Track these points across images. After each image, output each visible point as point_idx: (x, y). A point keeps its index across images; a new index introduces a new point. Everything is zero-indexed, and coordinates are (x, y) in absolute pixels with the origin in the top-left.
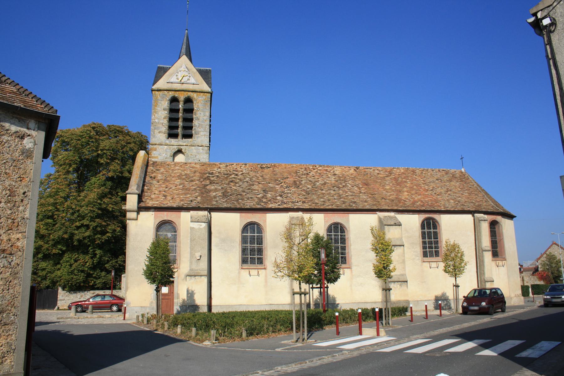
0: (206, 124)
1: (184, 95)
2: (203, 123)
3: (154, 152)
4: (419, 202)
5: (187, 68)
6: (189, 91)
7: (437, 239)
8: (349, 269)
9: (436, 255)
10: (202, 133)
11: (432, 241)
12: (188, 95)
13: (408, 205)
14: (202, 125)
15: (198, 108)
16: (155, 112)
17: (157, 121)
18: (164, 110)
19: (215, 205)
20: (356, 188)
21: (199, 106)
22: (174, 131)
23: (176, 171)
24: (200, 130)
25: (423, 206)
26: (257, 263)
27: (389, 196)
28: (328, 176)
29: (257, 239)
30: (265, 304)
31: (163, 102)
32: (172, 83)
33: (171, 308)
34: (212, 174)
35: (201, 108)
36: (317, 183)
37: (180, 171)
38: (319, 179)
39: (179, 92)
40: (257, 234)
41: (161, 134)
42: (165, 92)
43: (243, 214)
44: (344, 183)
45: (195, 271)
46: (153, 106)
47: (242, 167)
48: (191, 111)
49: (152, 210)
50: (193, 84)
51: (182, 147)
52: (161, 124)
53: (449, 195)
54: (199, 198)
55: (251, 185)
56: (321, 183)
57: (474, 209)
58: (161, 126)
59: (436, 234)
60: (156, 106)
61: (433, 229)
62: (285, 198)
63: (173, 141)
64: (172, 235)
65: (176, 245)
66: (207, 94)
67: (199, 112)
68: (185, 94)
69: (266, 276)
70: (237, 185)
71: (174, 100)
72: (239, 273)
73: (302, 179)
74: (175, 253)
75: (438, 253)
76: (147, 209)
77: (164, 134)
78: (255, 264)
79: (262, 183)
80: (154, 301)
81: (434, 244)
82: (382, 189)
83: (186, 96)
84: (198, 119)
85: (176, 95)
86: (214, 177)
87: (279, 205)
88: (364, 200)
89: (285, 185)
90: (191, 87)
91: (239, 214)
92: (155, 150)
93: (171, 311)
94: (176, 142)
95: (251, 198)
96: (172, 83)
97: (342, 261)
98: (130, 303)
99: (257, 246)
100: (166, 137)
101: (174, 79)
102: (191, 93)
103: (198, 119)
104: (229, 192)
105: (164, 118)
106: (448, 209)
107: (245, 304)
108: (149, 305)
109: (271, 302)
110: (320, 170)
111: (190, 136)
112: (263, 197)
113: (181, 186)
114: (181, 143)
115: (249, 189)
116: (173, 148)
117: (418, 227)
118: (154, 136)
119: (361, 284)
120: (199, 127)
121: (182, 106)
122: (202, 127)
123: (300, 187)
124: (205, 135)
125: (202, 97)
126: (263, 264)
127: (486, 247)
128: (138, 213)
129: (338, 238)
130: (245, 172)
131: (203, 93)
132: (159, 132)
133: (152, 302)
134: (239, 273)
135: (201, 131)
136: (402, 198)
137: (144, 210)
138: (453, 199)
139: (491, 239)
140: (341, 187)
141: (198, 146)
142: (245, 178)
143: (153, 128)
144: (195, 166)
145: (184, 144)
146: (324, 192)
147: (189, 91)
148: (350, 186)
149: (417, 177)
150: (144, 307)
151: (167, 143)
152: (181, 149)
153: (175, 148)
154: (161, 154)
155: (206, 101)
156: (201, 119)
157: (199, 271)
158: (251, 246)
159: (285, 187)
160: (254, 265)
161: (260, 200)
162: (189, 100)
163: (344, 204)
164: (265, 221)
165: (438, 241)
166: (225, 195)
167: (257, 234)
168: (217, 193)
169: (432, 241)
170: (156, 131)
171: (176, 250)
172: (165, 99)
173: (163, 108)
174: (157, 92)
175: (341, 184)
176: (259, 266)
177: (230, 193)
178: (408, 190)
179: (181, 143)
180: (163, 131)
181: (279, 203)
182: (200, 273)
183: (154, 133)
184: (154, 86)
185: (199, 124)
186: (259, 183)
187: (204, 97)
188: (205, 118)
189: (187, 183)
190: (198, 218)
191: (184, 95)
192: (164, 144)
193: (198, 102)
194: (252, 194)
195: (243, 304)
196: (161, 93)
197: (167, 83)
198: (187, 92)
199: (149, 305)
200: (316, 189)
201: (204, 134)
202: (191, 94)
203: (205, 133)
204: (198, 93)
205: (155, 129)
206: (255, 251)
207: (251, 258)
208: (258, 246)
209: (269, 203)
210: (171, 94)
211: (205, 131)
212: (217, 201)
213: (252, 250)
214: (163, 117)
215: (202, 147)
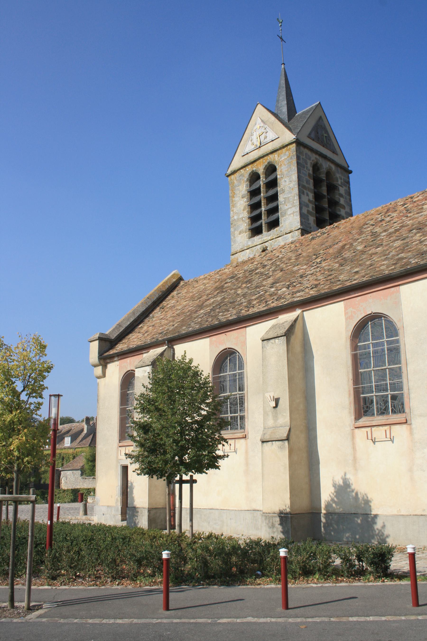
1: (263, 163)
6: (267, 155)
8: (405, 426)
10: (290, 212)
12: (268, 161)
14: (289, 197)
15: (282, 174)
16: (233, 206)
17: (236, 217)
18: (243, 198)
21: (283, 170)
22: (258, 224)
30: (246, 509)
31: (240, 187)
32: (247, 154)
35: (285, 173)
39: (257, 162)
41: (242, 235)
42: (242, 170)
43: (214, 338)
46: (230, 198)
49: (116, 359)
50: (272, 141)
51: (266, 244)
52: (241, 221)
58: (241, 222)
60: (233, 197)
63: (256, 240)
66: (291, 146)
67: (283, 180)
68: (264, 161)
69: (247, 452)
76: (111, 358)
77: (246, 232)
83: (266, 163)
84: (283, 191)
85: (254, 169)
91: (208, 340)
94: (259, 239)
96: (247, 154)
97: (394, 406)
100: (248, 236)
102: (271, 156)
105: (244, 210)
107: (218, 507)
108: (114, 505)
114: (265, 238)
116: (256, 249)
120: (285, 203)
121: (263, 181)
124: (293, 213)
125: (285, 155)
128: (105, 367)
129: (383, 350)
131: (285, 148)
135: (288, 209)
141: (286, 234)
143: (233, 230)
145: (269, 238)
147: (267, 155)
150: (110, 506)
151: (249, 245)
152: (267, 247)
153: (259, 248)
155: (291, 158)
156: (287, 189)
164: (244, 343)
170: (237, 233)
172: (242, 182)
173: (241, 196)
174: (232, 177)
180: (244, 229)
183: (234, 237)
184: (229, 170)
185: (285, 198)
187: (287, 153)
191: (263, 163)
192: (246, 248)
193: (281, 165)
195: (215, 508)
196: (237, 175)
197: (243, 156)
198: (266, 158)
199: (114, 505)
202: (271, 158)
204: (280, 151)
205: (235, 230)
214: (242, 208)
215: (291, 234)
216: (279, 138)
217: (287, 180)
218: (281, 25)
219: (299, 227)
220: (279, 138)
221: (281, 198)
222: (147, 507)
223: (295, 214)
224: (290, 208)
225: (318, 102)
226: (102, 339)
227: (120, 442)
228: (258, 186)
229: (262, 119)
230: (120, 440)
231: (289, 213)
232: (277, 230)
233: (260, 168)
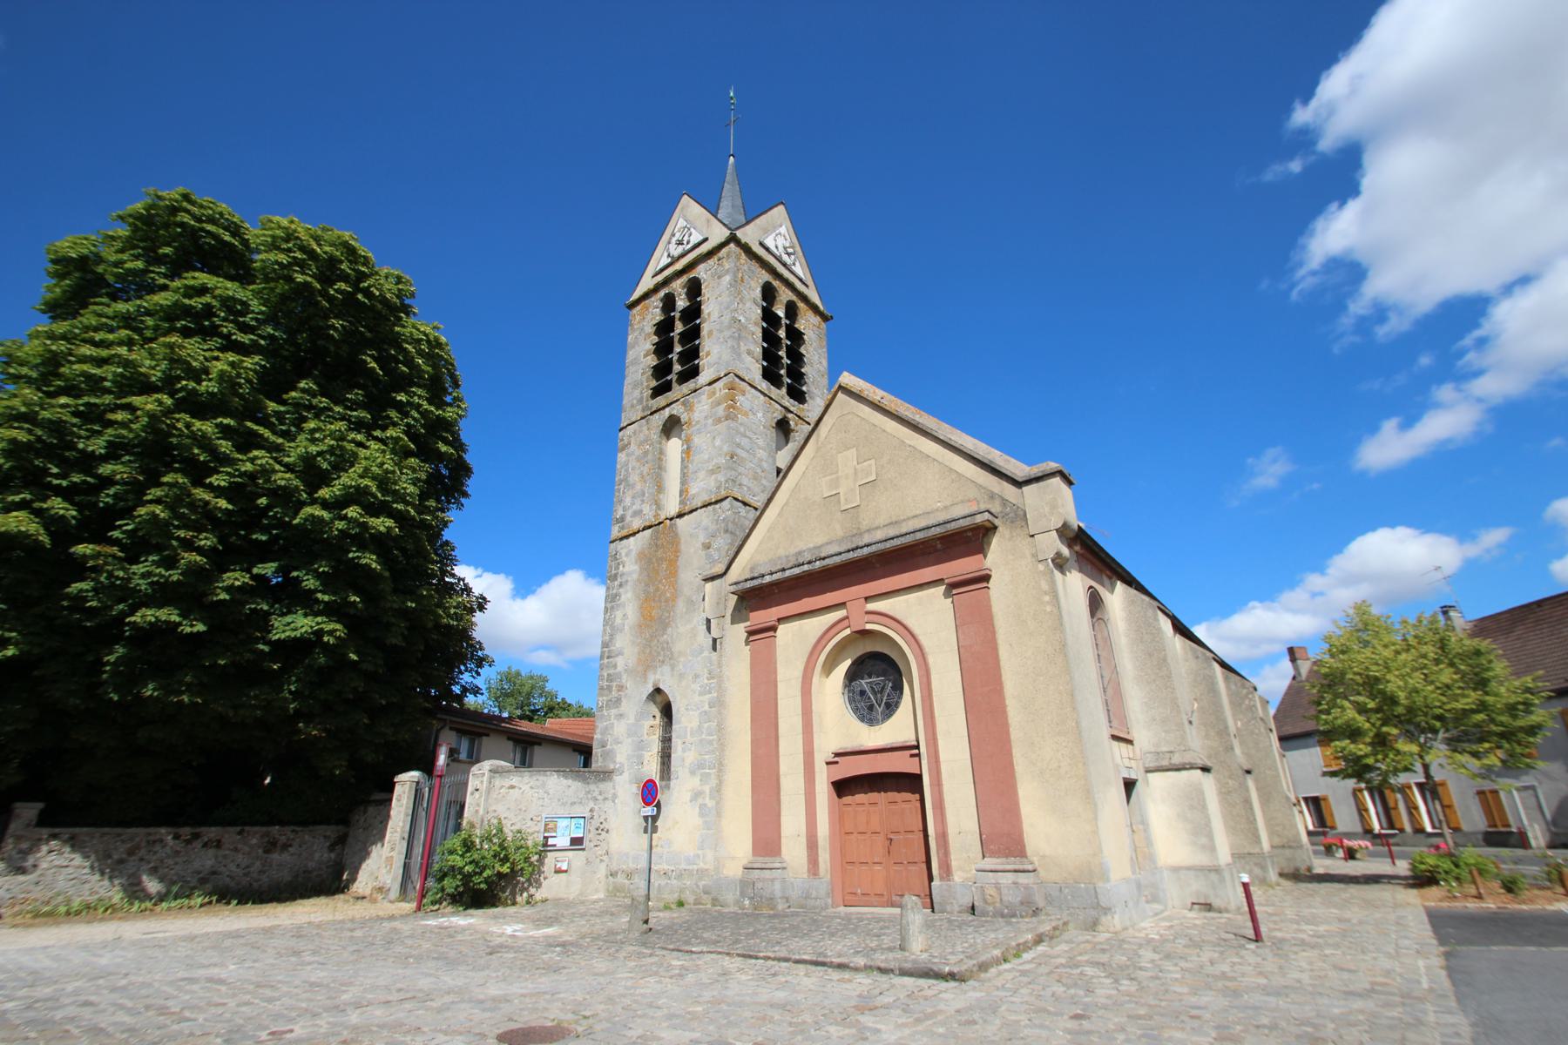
101: (769, 242)
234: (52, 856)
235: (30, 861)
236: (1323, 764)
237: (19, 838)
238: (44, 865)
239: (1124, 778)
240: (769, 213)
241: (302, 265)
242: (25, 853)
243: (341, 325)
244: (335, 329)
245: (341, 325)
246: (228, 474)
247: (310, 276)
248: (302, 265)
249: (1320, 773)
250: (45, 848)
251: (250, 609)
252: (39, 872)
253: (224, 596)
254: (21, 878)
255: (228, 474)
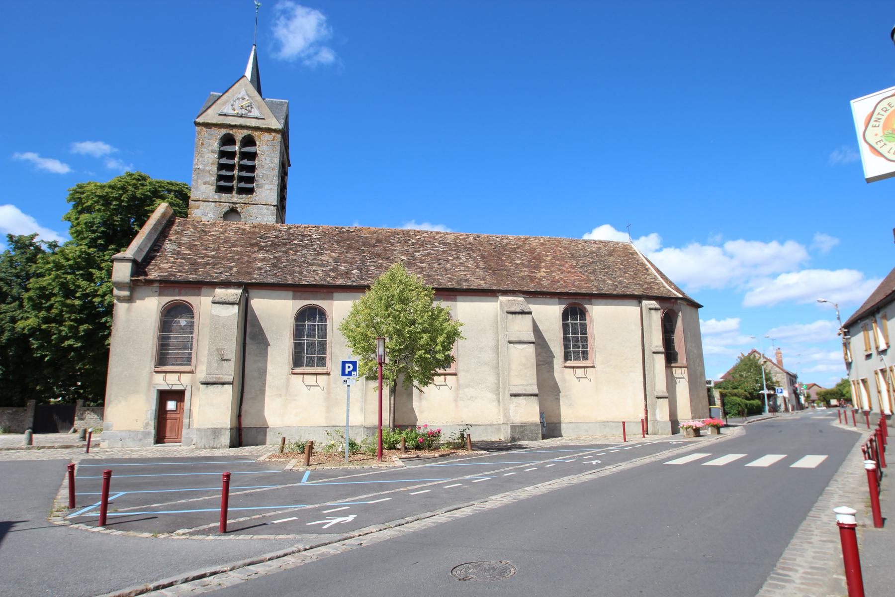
0: (273, 174)
2: (269, 173)
3: (196, 211)
4: (562, 282)
5: (248, 95)
7: (586, 334)
8: (454, 377)
9: (583, 357)
10: (267, 187)
11: (578, 338)
13: (546, 286)
19: (255, 279)
20: (472, 262)
23: (213, 233)
24: (265, 182)
25: (566, 287)
26: (317, 366)
27: (518, 273)
28: (434, 245)
29: (318, 329)
33: (180, 432)
34: (266, 238)
36: (417, 254)
37: (218, 233)
38: (420, 249)
40: (319, 322)
44: (456, 254)
45: (214, 376)
47: (311, 231)
48: (253, 156)
53: (606, 273)
54: (235, 269)
55: (318, 254)
56: (423, 253)
57: (640, 293)
59: (584, 327)
61: (580, 320)
62: (365, 271)
64: (188, 322)
65: (192, 337)
70: (299, 253)
71: (228, 140)
72: (288, 379)
73: (395, 247)
74: (191, 350)
75: (587, 354)
77: (212, 185)
78: (315, 366)
79: (336, 251)
80: (150, 422)
81: (581, 342)
82: (509, 263)
84: (262, 167)
86: (267, 242)
87: (353, 281)
88: (480, 279)
89: (369, 255)
90: (253, 123)
92: (198, 207)
93: (179, 437)
95: (314, 271)
98: (112, 426)
99: (317, 341)
100: (215, 190)
101: (228, 110)
103: (262, 167)
104: (283, 263)
105: (212, 164)
106: (603, 292)
107: (295, 426)
109: (333, 423)
110: (424, 237)
111: (251, 191)
112: (332, 270)
113: (213, 253)
115: (314, 259)
117: (558, 317)
118: (197, 187)
119: (472, 397)
122: (267, 178)
123: (391, 258)
126: (325, 366)
127: (657, 346)
130: (315, 237)
132: (205, 183)
133: (147, 424)
134: (288, 379)
136: (537, 276)
137: (142, 284)
138: (611, 280)
139: (665, 336)
140: (451, 260)
142: (312, 245)
144: (243, 227)
146: (424, 265)
148: (464, 258)
149: (562, 249)
154: (206, 214)
157: (221, 376)
158: (308, 340)
159: (368, 258)
160: (313, 368)
161: (327, 274)
162: (249, 141)
163: (449, 281)
165: (587, 337)
166: (275, 266)
167: (319, 322)
168: (264, 263)
169: (578, 338)
171: (192, 344)
175: (451, 256)
176: (319, 370)
177: (284, 264)
178: (547, 266)
179: (235, 200)
181: (353, 279)
182: (222, 379)
186: (332, 252)
188: (272, 165)
189: (224, 249)
190: (224, 298)
192: (210, 200)
194: (317, 266)
200: (414, 262)
201: (270, 188)
203: (271, 186)
206: (314, 347)
207: (307, 357)
208: (320, 341)
209: (340, 277)
210: (223, 131)
211: (271, 182)
212: (260, 275)
213: (311, 346)
214: (211, 161)
216: (264, 119)
217: (268, 159)
218: (257, 8)
219: (276, 203)
220: (264, 119)
221: (258, 173)
222: (229, 426)
223: (272, 191)
224: (268, 184)
225: (288, 101)
226: (134, 261)
227: (155, 368)
228: (234, 150)
229: (248, 92)
230: (155, 365)
231: (266, 188)
232: (250, 197)
233: (239, 135)
234: (88, 415)
235: (84, 417)
236: (865, 349)
237: (80, 410)
238: (87, 418)
239: (158, 390)
240: (231, 90)
241: (97, 202)
242: (82, 414)
243: (120, 218)
244: (117, 221)
245: (120, 218)
246: (81, 291)
247: (101, 205)
248: (97, 202)
249: (864, 357)
250: (86, 413)
251: (101, 335)
252: (86, 420)
253: (83, 333)
254: (82, 421)
255: (81, 291)
